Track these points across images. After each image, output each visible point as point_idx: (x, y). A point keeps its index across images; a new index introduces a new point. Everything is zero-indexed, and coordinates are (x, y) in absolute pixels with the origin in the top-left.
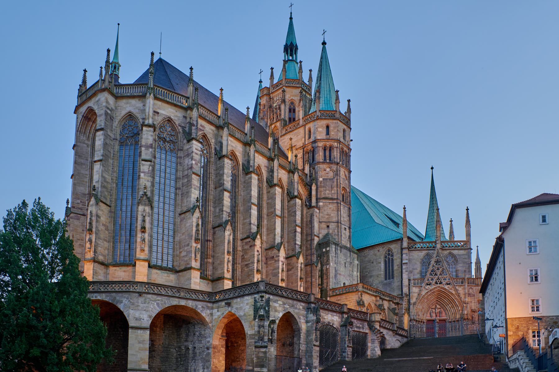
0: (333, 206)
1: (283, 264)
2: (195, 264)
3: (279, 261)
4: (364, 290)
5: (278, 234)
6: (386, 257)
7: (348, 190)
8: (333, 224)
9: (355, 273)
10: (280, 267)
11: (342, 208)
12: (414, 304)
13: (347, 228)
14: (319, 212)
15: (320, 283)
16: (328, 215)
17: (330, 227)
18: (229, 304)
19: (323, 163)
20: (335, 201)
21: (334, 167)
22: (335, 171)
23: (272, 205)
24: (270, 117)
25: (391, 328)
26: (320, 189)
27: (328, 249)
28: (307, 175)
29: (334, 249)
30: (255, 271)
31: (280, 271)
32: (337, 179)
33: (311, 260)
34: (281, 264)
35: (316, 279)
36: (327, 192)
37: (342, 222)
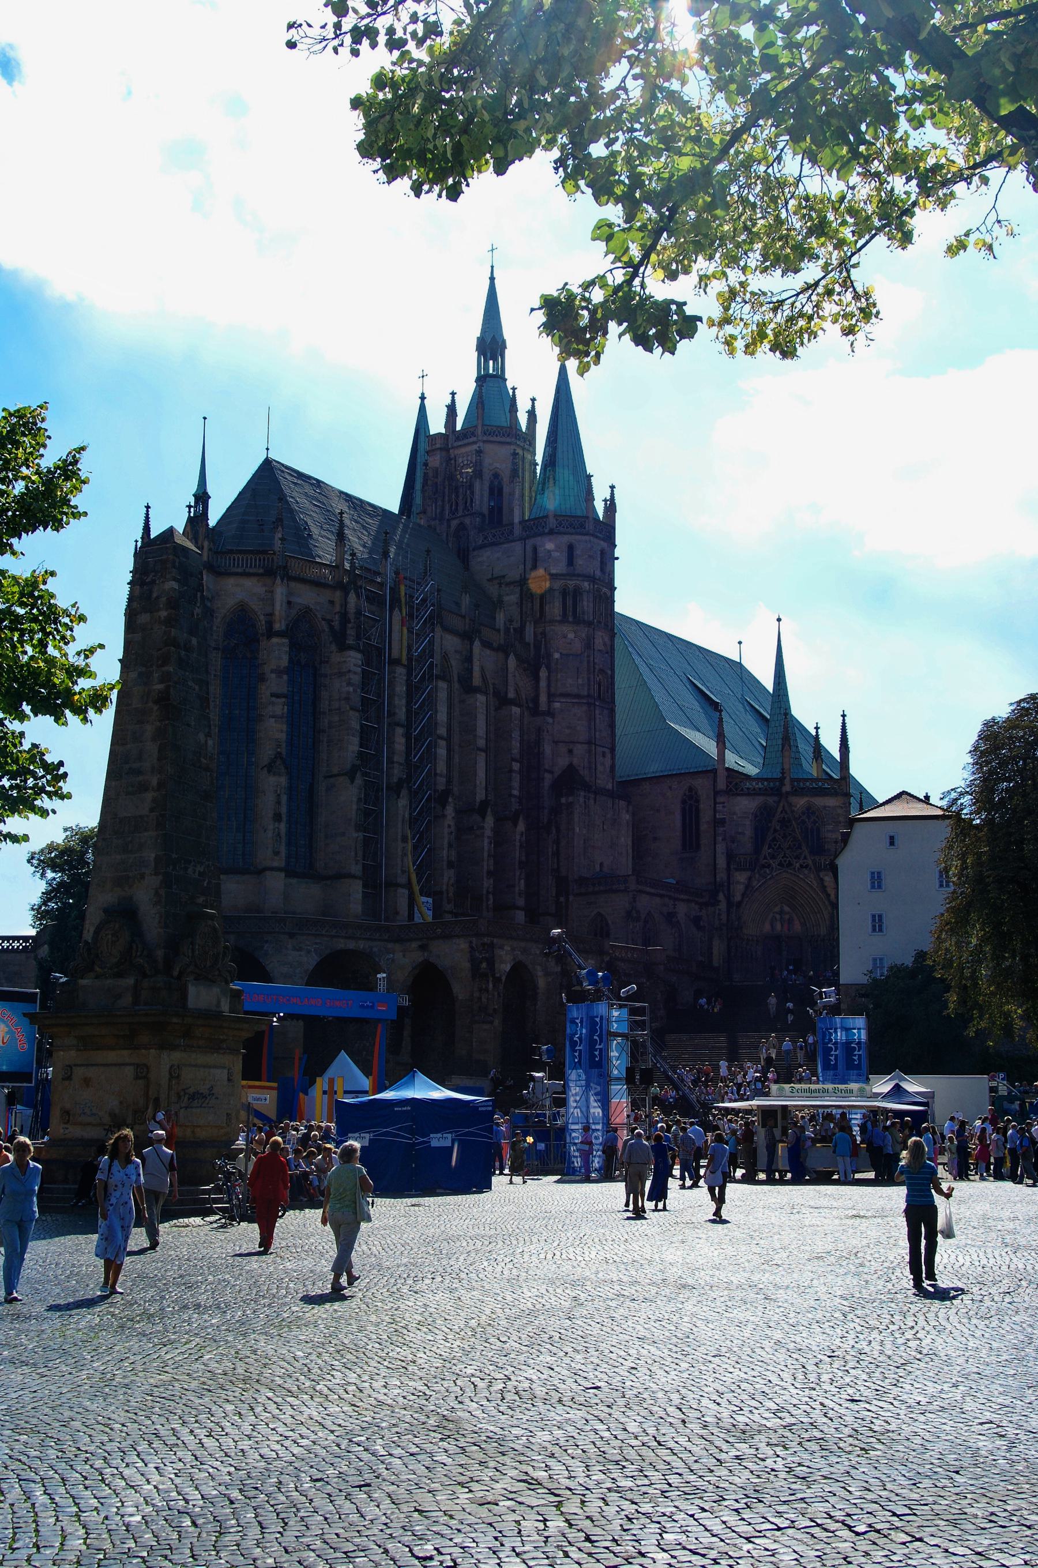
2: (356, 869)
4: (640, 887)
6: (684, 802)
8: (579, 746)
10: (486, 848)
11: (597, 712)
12: (739, 904)
15: (555, 866)
18: (423, 948)
19: (561, 622)
24: (449, 501)
27: (571, 799)
28: (529, 644)
29: (582, 800)
30: (445, 863)
31: (486, 854)
32: (588, 656)
34: (486, 841)
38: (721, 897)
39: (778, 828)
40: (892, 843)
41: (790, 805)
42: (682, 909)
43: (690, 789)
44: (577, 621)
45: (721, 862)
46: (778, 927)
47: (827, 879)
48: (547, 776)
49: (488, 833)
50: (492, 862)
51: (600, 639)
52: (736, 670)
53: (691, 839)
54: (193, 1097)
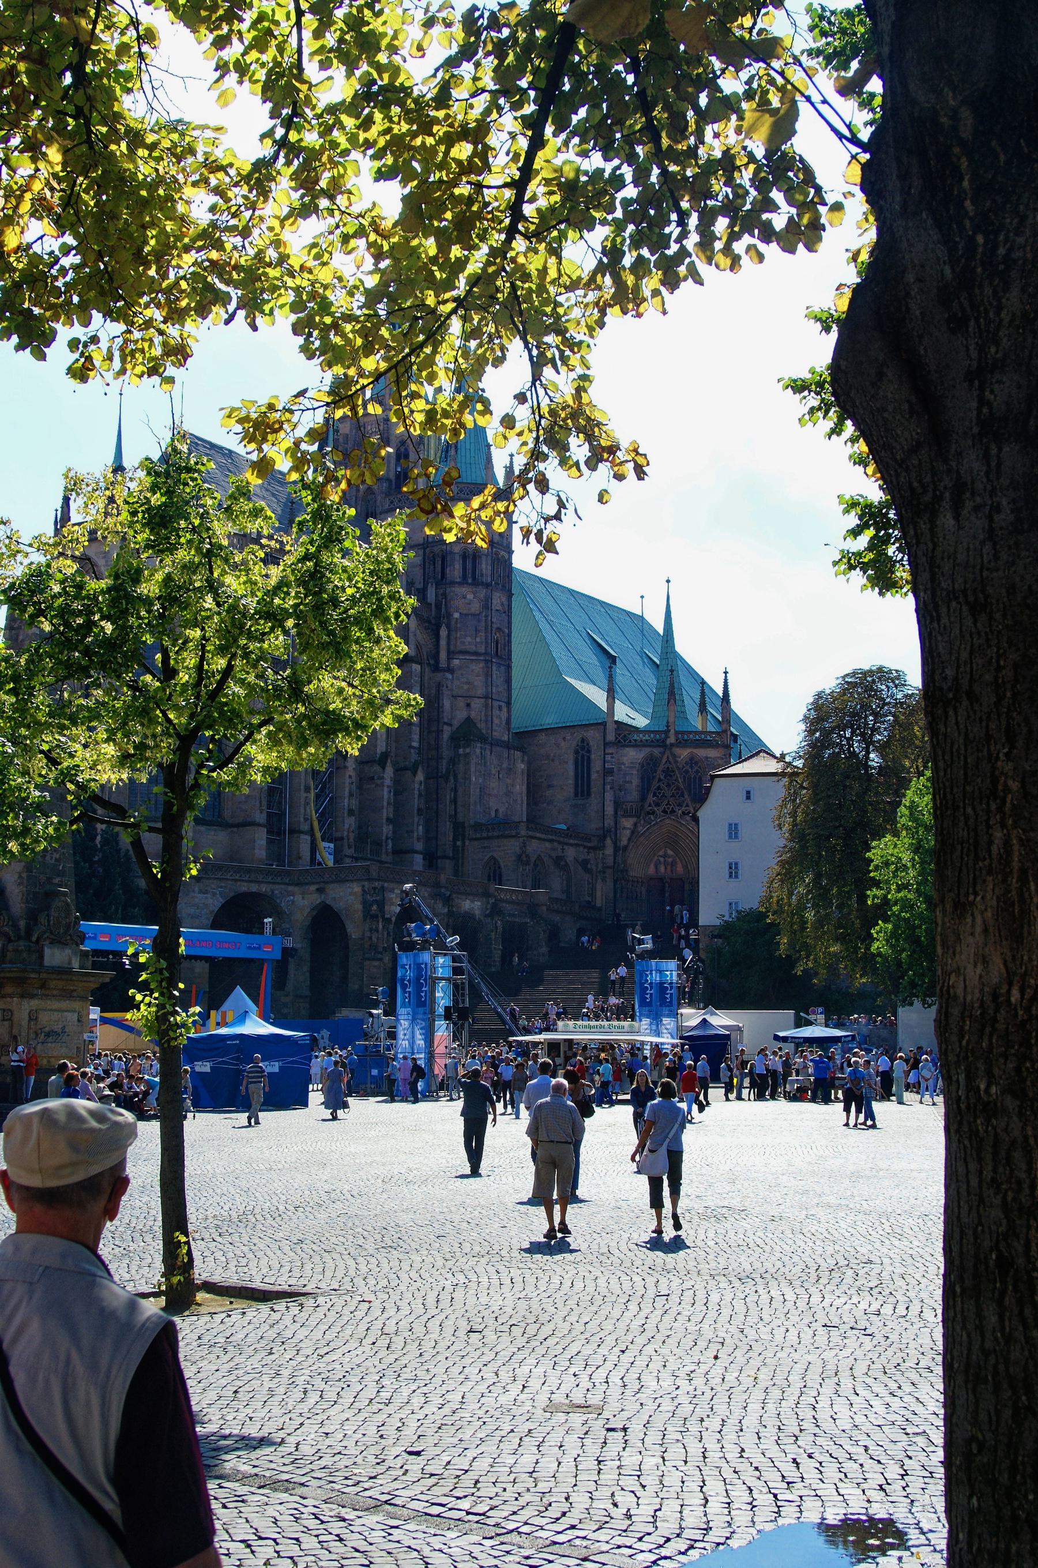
0: (478, 667)
2: (261, 818)
6: (577, 752)
8: (477, 701)
10: (386, 797)
12: (625, 848)
16: (468, 683)
17: (473, 705)
18: (320, 891)
19: (460, 584)
21: (482, 593)
26: (453, 633)
27: (468, 750)
29: (478, 751)
34: (386, 789)
36: (469, 639)
38: (608, 842)
40: (748, 798)
41: (674, 756)
42: (571, 853)
43: (583, 740)
44: (476, 583)
45: (610, 809)
46: (662, 869)
48: (446, 728)
49: (388, 782)
50: (391, 809)
51: (498, 599)
52: (639, 621)
53: (582, 787)
54: (48, 1035)
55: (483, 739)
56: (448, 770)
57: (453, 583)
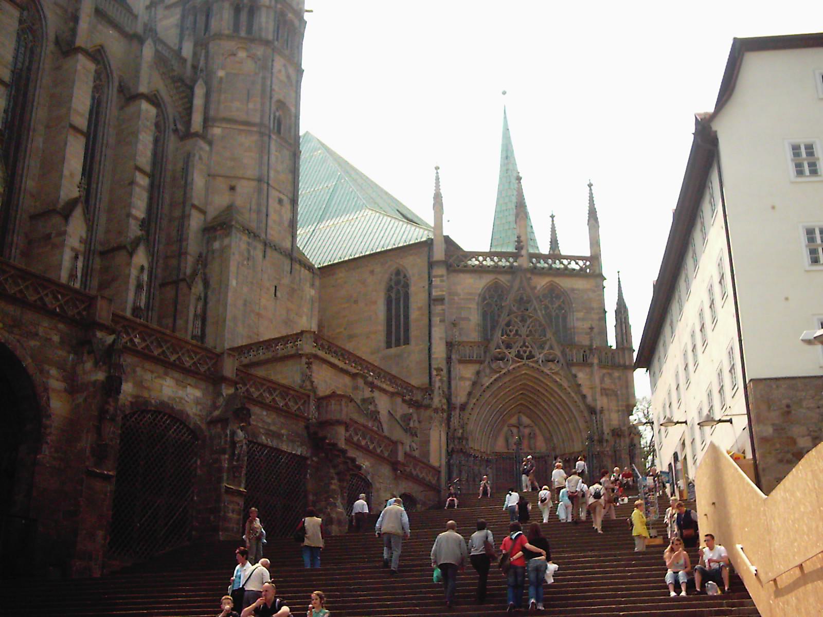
1: (76, 257)
3: (62, 245)
5: (72, 175)
6: (389, 289)
7: (293, 110)
9: (305, 318)
12: (463, 407)
13: (286, 200)
14: (211, 150)
17: (239, 189)
19: (229, 37)
20: (255, 129)
22: (259, 59)
23: (61, 101)
25: (386, 454)
26: (214, 97)
27: (226, 241)
28: (185, 60)
29: (243, 246)
32: (264, 78)
33: (179, 269)
34: (67, 256)
35: (187, 322)
37: (270, 182)
39: (515, 309)
43: (398, 273)
45: (439, 351)
47: (581, 375)
55: (253, 234)
56: (195, 273)
57: (219, 36)
